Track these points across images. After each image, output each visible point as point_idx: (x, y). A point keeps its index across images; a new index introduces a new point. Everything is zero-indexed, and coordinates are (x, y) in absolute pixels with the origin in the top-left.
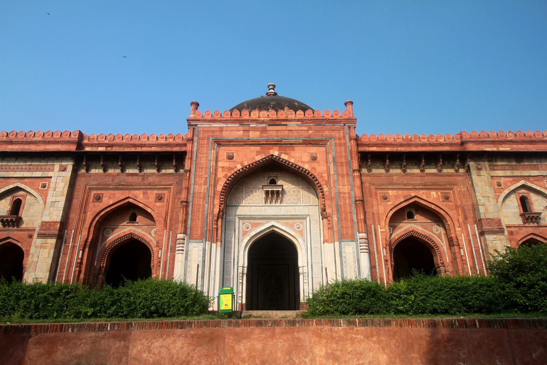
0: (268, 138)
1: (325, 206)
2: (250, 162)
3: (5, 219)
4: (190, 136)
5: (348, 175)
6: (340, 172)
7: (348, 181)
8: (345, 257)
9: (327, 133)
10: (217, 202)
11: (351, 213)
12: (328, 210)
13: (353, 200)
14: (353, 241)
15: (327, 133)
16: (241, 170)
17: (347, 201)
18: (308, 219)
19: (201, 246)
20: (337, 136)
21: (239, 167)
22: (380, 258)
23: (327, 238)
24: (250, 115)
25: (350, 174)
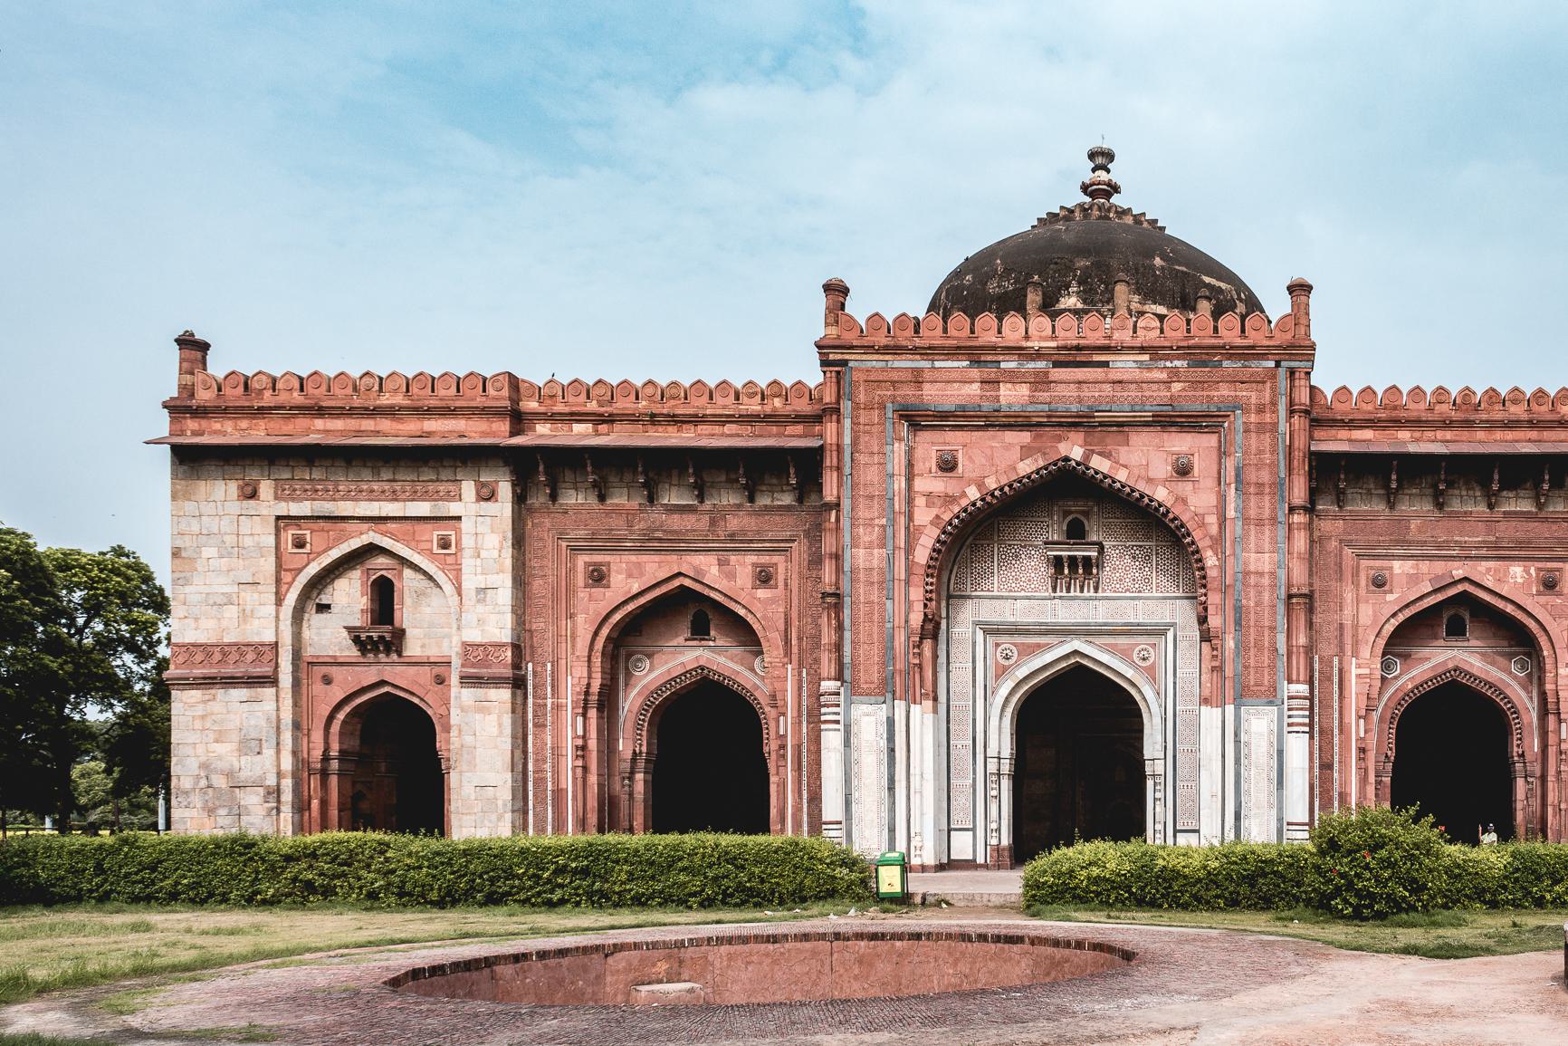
0: (1053, 406)
1: (1206, 609)
2: (1004, 481)
3: (363, 636)
4: (829, 397)
5: (1274, 520)
6: (1252, 513)
7: (1274, 541)
8: (1247, 744)
9: (1225, 391)
10: (917, 594)
11: (1273, 629)
12: (1214, 621)
13: (1283, 593)
14: (1271, 703)
15: (1225, 391)
16: (979, 504)
17: (1266, 596)
18: (1170, 635)
19: (882, 712)
20: (1253, 401)
21: (973, 494)
22: (1345, 745)
23: (1206, 693)
24: (1000, 332)
25: (1281, 518)
